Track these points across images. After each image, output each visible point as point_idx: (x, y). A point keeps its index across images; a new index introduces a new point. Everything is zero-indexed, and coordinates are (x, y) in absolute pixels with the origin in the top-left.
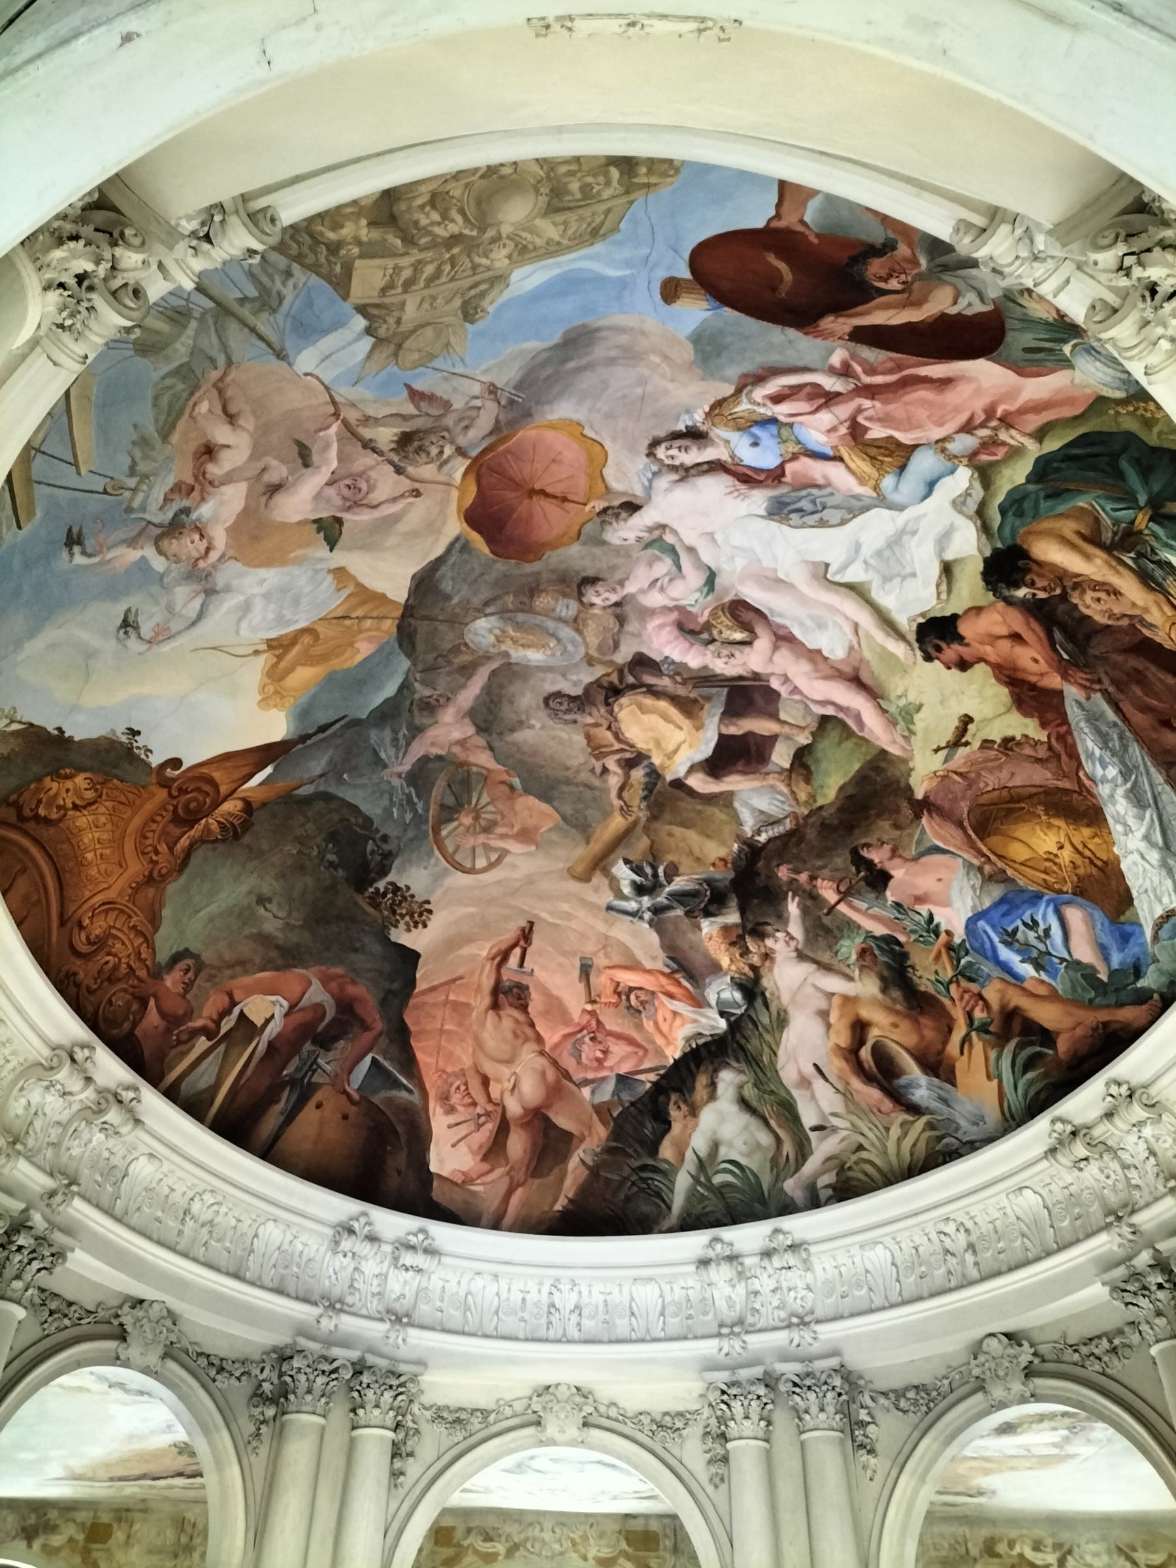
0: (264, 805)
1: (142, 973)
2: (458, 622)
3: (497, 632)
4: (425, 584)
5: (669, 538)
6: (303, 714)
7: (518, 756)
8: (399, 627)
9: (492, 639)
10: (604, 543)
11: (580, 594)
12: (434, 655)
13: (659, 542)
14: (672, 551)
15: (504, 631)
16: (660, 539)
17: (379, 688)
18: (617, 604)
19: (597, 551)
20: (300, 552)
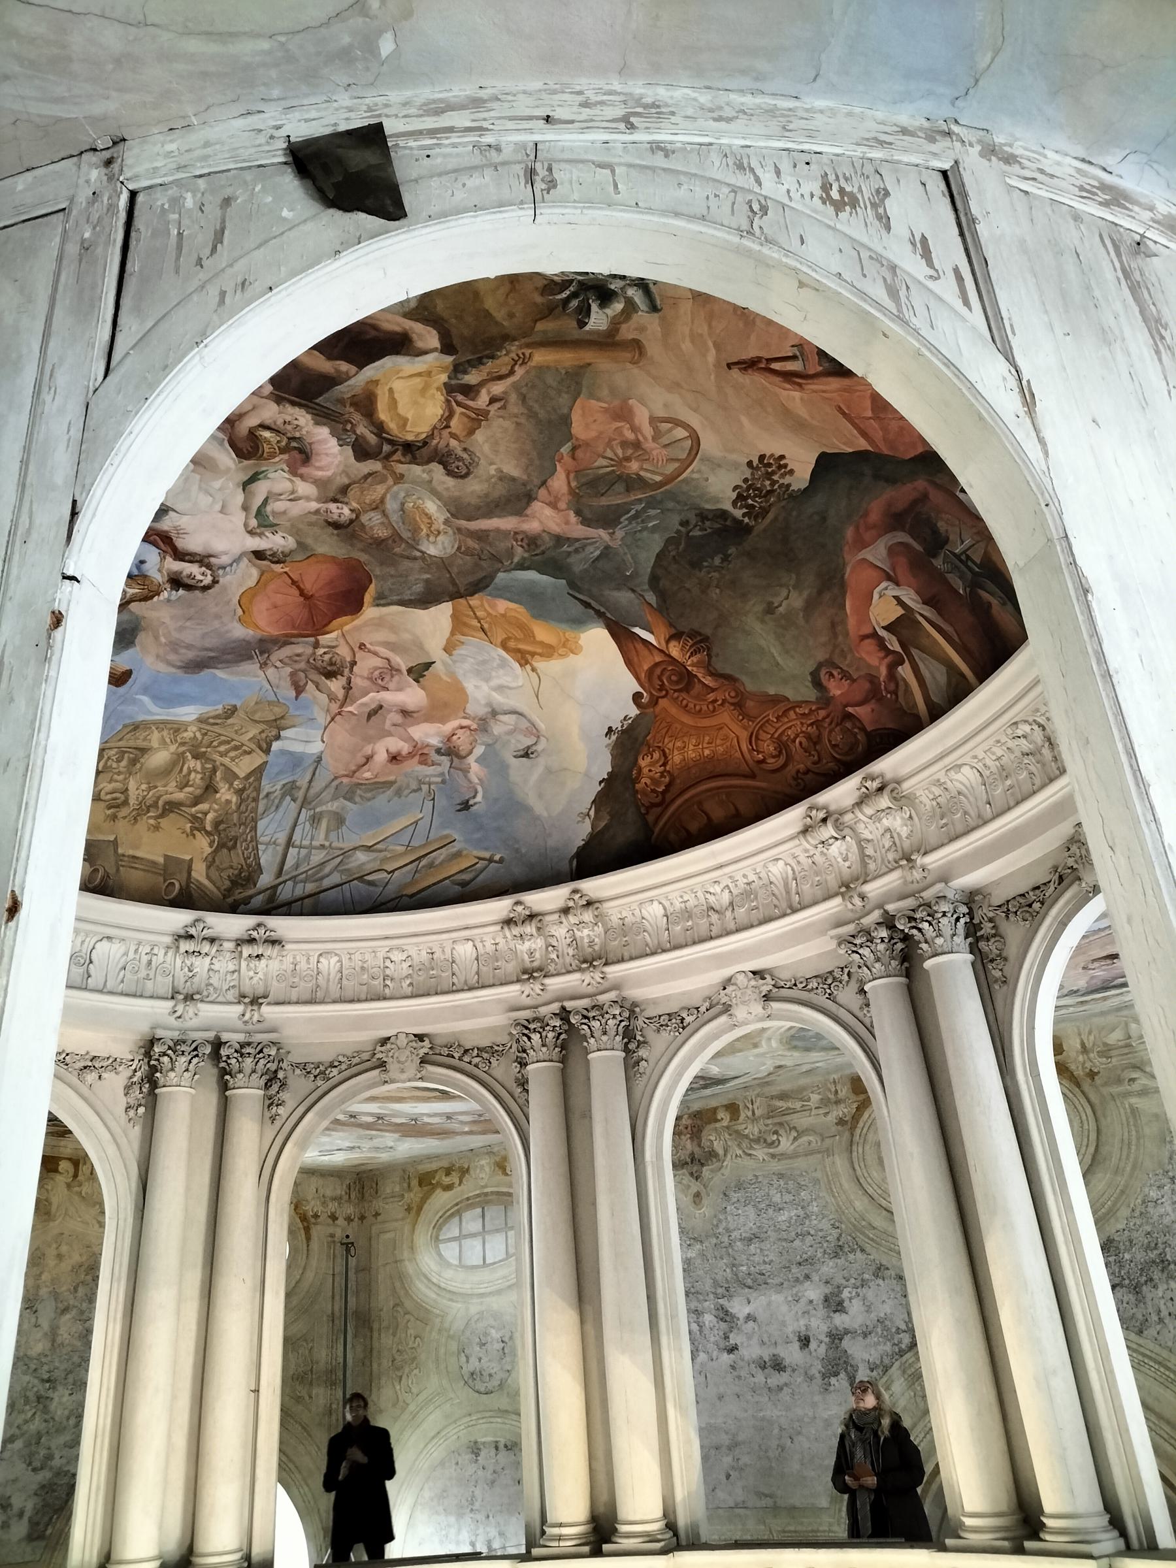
0: (671, 625)
1: (822, 713)
2: (443, 564)
3: (432, 539)
4: (426, 600)
5: (253, 523)
6: (579, 623)
7: (537, 462)
8: (472, 595)
9: (440, 538)
10: (299, 543)
11: (352, 521)
12: (482, 563)
13: (263, 521)
14: (259, 513)
15: (428, 535)
16: (260, 526)
17: (533, 582)
18: (335, 500)
19: (309, 541)
20: (445, 678)
